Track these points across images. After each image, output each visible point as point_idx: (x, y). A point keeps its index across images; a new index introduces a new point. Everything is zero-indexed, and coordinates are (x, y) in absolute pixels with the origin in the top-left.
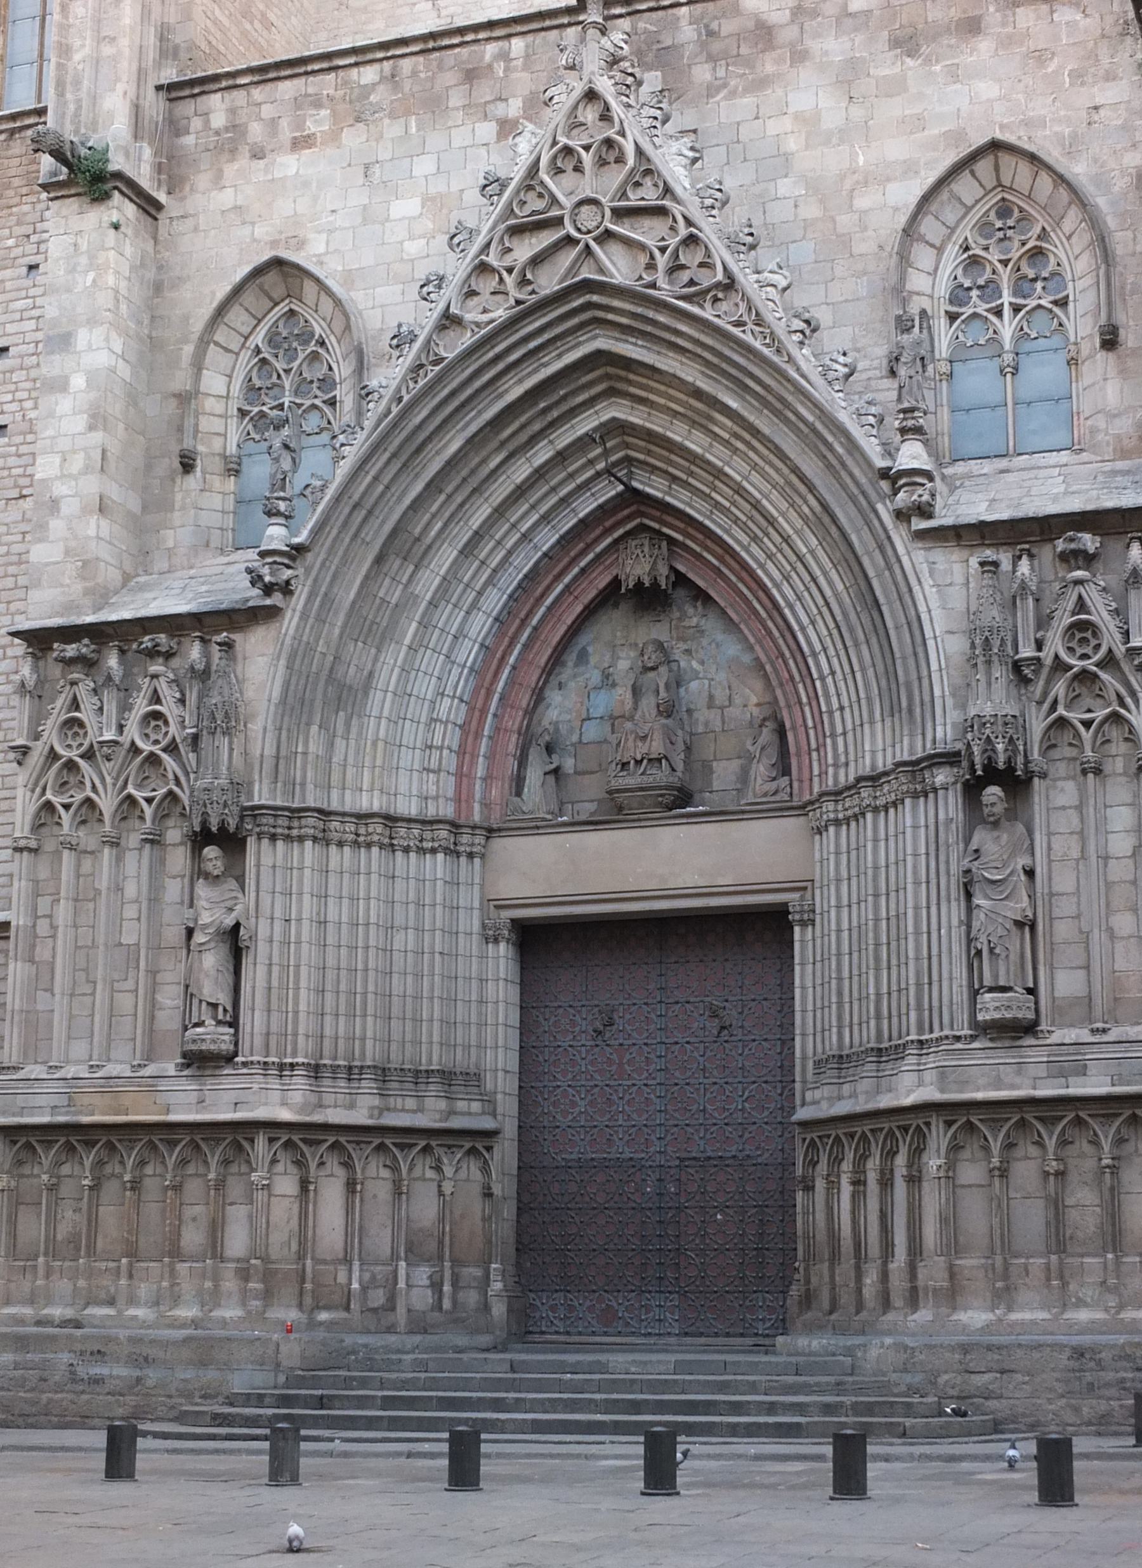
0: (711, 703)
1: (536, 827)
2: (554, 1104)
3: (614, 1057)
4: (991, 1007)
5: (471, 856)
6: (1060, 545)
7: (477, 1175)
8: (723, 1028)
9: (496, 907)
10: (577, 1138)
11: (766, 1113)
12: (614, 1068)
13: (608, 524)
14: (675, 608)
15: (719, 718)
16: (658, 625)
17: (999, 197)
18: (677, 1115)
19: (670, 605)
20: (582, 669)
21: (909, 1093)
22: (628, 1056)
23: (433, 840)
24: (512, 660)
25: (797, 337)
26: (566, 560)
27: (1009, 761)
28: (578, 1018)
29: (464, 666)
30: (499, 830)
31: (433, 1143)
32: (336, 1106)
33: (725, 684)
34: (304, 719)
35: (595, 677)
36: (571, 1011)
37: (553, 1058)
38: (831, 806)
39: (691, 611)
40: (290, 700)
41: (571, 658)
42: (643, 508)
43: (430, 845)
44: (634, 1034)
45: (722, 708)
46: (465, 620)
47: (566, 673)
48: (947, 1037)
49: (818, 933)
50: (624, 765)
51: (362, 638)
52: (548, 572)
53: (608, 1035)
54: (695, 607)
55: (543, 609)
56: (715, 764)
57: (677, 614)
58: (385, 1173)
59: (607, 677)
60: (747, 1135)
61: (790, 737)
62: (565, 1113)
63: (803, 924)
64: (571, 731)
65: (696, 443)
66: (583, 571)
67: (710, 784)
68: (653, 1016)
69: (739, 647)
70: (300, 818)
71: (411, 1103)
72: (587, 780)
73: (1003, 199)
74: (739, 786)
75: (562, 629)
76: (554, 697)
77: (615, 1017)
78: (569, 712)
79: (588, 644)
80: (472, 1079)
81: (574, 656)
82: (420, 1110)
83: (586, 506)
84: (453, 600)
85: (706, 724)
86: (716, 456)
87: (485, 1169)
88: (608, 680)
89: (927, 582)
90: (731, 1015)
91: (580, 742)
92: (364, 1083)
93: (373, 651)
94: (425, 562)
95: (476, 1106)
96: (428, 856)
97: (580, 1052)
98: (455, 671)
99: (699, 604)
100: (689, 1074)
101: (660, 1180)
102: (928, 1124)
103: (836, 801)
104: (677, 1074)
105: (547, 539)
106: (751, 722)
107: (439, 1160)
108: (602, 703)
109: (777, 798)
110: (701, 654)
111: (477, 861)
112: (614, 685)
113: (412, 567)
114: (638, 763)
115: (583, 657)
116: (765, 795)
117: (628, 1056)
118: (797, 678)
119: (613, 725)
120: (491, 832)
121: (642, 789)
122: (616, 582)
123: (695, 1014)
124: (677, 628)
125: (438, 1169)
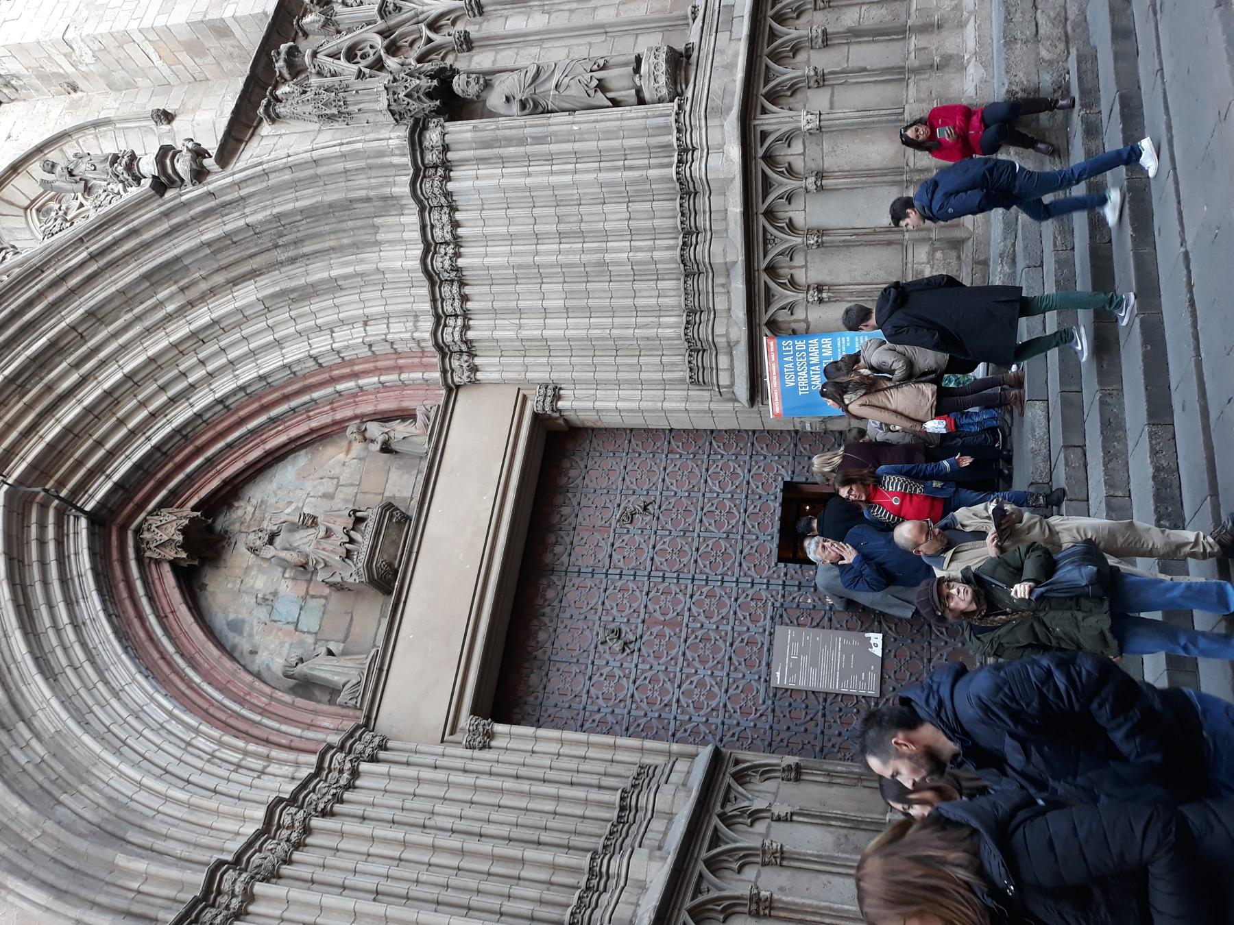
0: (329, 496)
1: (380, 669)
2: (698, 708)
3: (655, 630)
4: (655, 79)
5: (383, 747)
6: (280, 65)
7: (771, 785)
8: (645, 509)
9: (452, 733)
10: (741, 684)
11: (739, 471)
12: (667, 631)
13: (115, 554)
14: (231, 527)
15: (345, 489)
16: (238, 544)
17: (34, 210)
18: (729, 564)
19: (226, 532)
20: (247, 629)
21: (729, 160)
22: (658, 615)
23: (341, 771)
24: (197, 679)
25: (9, 256)
26: (128, 604)
27: (432, 77)
28: (605, 671)
29: (170, 714)
30: (368, 717)
31: (718, 809)
32: (638, 905)
33: (316, 482)
34: (102, 874)
35: (262, 613)
36: (595, 679)
37: (644, 705)
38: (448, 330)
39: (240, 512)
40: (62, 884)
41: (232, 638)
42: (119, 520)
43: (346, 775)
44: (635, 605)
45: (338, 485)
46: (125, 705)
47: (244, 645)
48: (677, 114)
49: (567, 375)
50: (349, 554)
51: (57, 793)
52: (129, 624)
53: (631, 637)
54: (238, 508)
55: (165, 641)
56: (387, 494)
57: (237, 527)
58: (750, 873)
59: (265, 600)
60: (760, 491)
61: (383, 406)
62: (711, 695)
63: (557, 397)
64: (301, 643)
65: (69, 413)
66: (151, 599)
67: (405, 499)
68: (619, 584)
69: (290, 468)
70: (219, 892)
71: (657, 825)
72: (356, 629)
73: (38, 210)
74: (415, 472)
75: (195, 627)
76: (262, 659)
77: (612, 626)
78: (282, 644)
79: (226, 618)
80: (644, 775)
81: (231, 635)
82: (670, 817)
83: (82, 562)
84: (90, 702)
85: (346, 501)
86: (90, 394)
87: (766, 772)
88: (268, 601)
89: (265, 158)
90: (635, 503)
91: (316, 633)
92: (613, 869)
93: (83, 788)
94: (28, 714)
95: (681, 766)
96: (358, 783)
97: (643, 672)
98: (173, 727)
99: (236, 504)
100: (686, 548)
101: (800, 586)
102: (764, 135)
103: (445, 325)
104: (685, 560)
105: (92, 605)
106: (360, 459)
107: (743, 812)
108: (287, 608)
109: (432, 414)
110: (281, 504)
111: (390, 744)
112: (275, 594)
113: (21, 726)
114: (352, 541)
115: (236, 626)
116: (426, 426)
117: (658, 615)
118: (329, 390)
119: (313, 597)
120: (368, 724)
121: (377, 534)
122: (174, 564)
123: (626, 538)
124: (249, 527)
125: (755, 816)
